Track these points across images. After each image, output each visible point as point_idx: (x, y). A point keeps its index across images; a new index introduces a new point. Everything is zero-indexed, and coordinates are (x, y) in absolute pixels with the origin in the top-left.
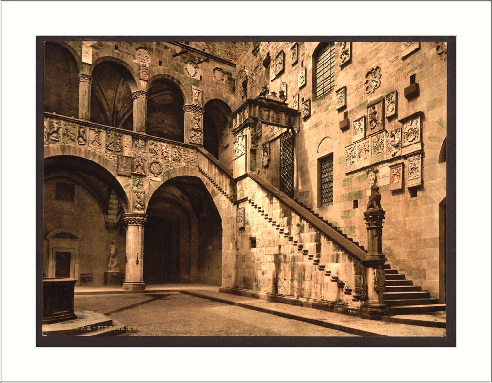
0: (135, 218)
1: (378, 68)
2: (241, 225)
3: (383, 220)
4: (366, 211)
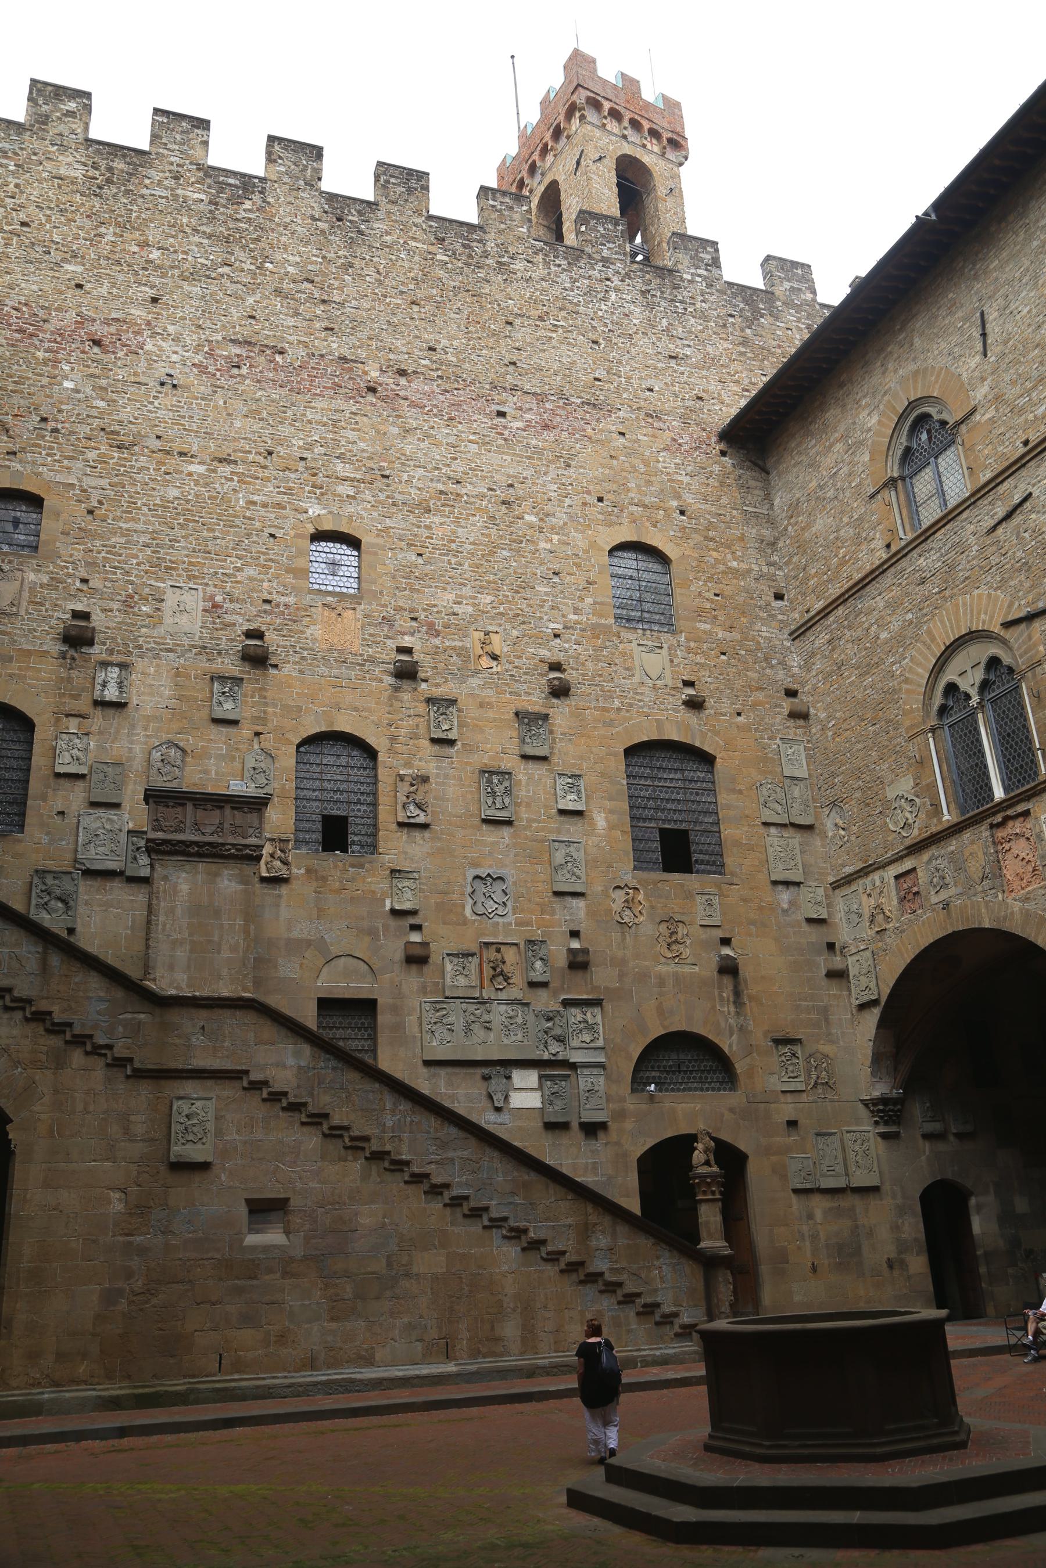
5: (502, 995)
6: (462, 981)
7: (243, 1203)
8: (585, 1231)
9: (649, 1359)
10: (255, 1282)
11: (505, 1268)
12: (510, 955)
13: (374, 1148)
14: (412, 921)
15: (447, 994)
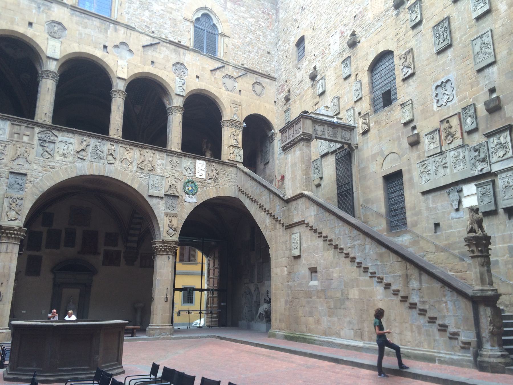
0: (166, 246)
1: (448, 81)
2: (297, 253)
3: (490, 247)
4: (466, 236)
5: (452, 146)
6: (432, 146)
7: (307, 269)
8: (407, 278)
9: (442, 359)
10: (311, 299)
11: (379, 298)
12: (454, 122)
13: (334, 244)
14: (412, 125)
15: (427, 155)
